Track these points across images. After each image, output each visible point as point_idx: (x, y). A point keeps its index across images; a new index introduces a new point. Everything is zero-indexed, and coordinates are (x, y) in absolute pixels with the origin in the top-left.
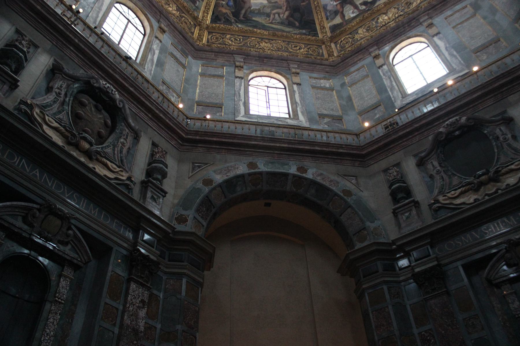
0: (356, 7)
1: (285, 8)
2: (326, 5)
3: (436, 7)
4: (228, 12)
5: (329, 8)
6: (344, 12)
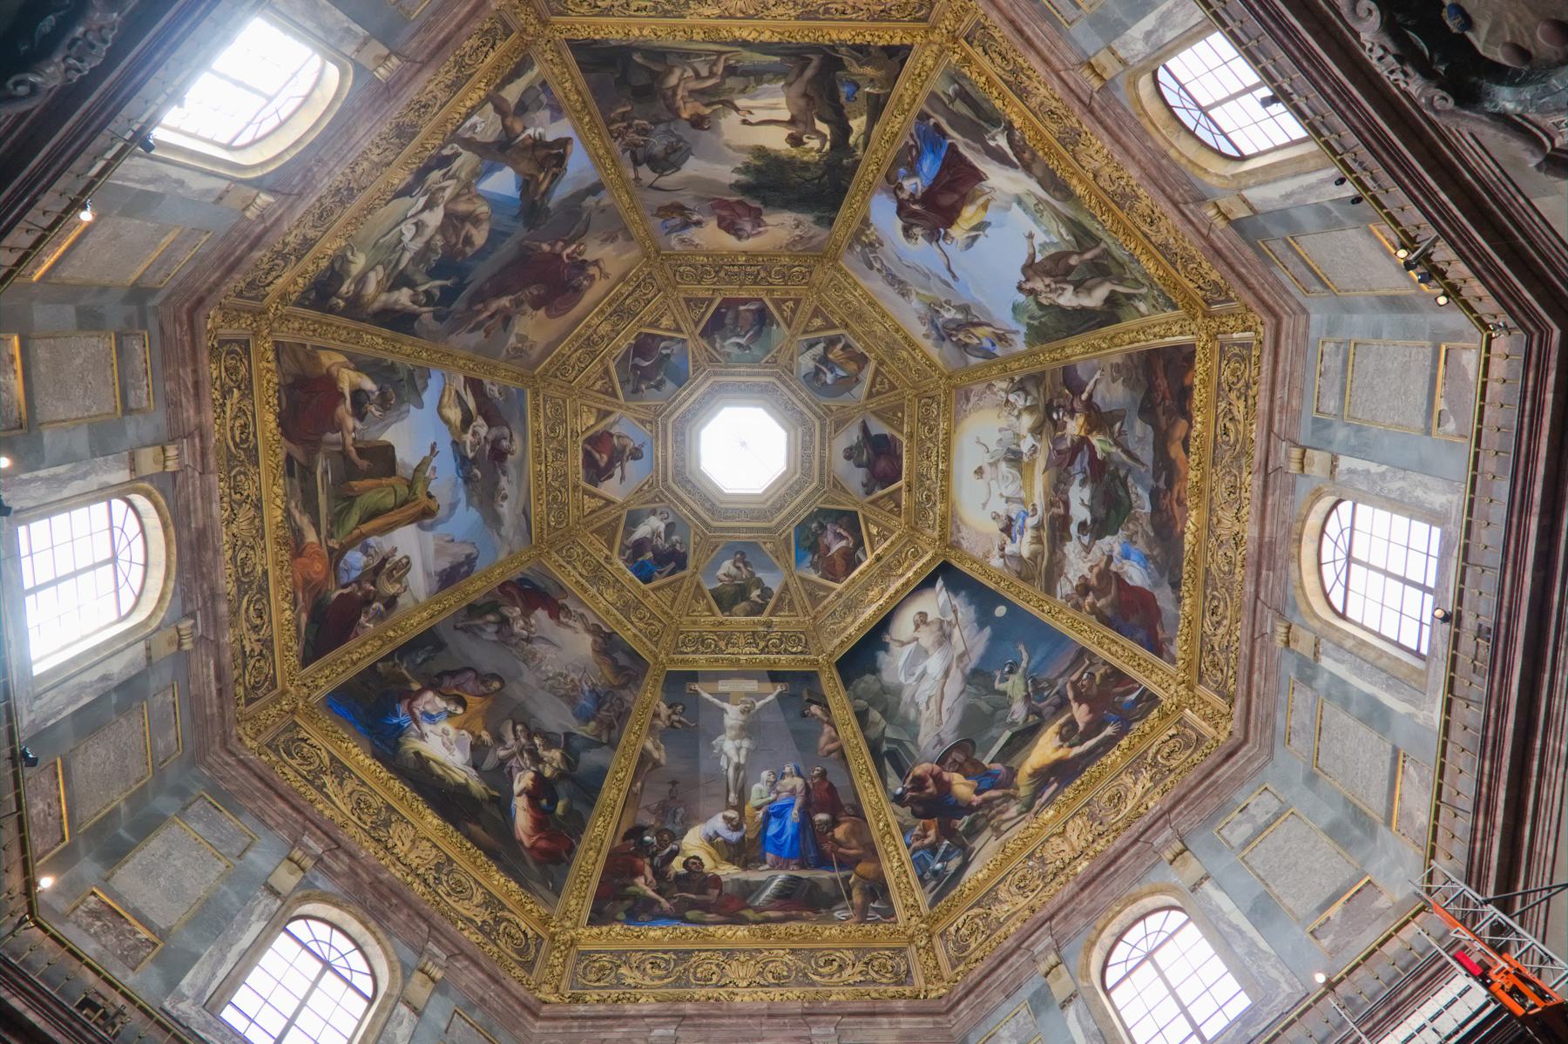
0: (469, 144)
1: (680, 93)
2: (554, 119)
3: (245, 245)
4: (855, 69)
5: (545, 114)
6: (499, 117)
